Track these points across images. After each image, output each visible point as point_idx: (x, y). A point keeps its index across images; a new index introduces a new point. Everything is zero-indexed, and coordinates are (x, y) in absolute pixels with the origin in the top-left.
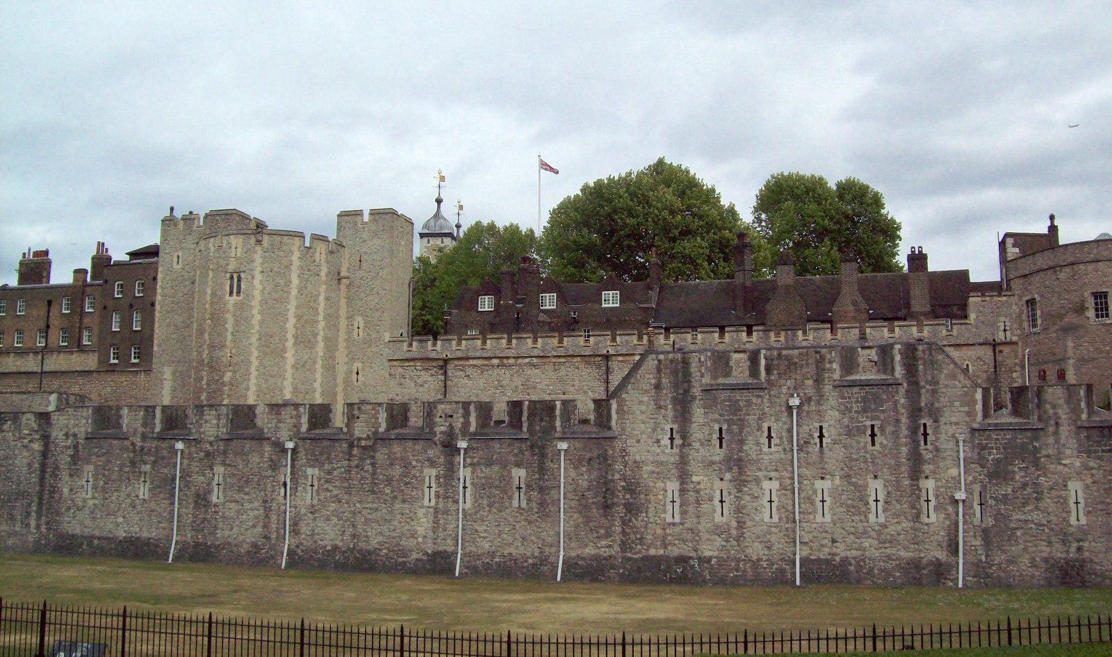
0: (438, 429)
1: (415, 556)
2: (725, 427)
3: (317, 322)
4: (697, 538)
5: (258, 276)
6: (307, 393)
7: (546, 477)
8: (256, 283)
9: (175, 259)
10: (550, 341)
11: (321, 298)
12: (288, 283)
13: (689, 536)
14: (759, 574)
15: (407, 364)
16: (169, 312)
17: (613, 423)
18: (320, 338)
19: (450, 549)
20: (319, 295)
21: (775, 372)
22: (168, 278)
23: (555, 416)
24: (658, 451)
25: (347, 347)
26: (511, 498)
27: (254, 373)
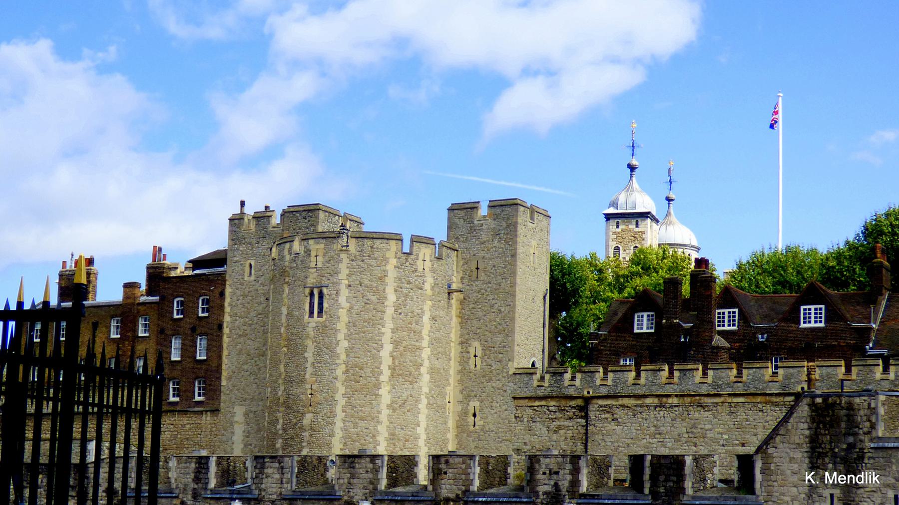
0: (542, 489)
3: (420, 349)
5: (344, 292)
6: (407, 441)
8: (342, 300)
9: (247, 269)
10: (723, 373)
11: (426, 318)
12: (382, 299)
15: (537, 403)
16: (240, 336)
17: (757, 486)
18: (423, 370)
20: (423, 313)
22: (238, 292)
25: (461, 381)
27: (340, 415)
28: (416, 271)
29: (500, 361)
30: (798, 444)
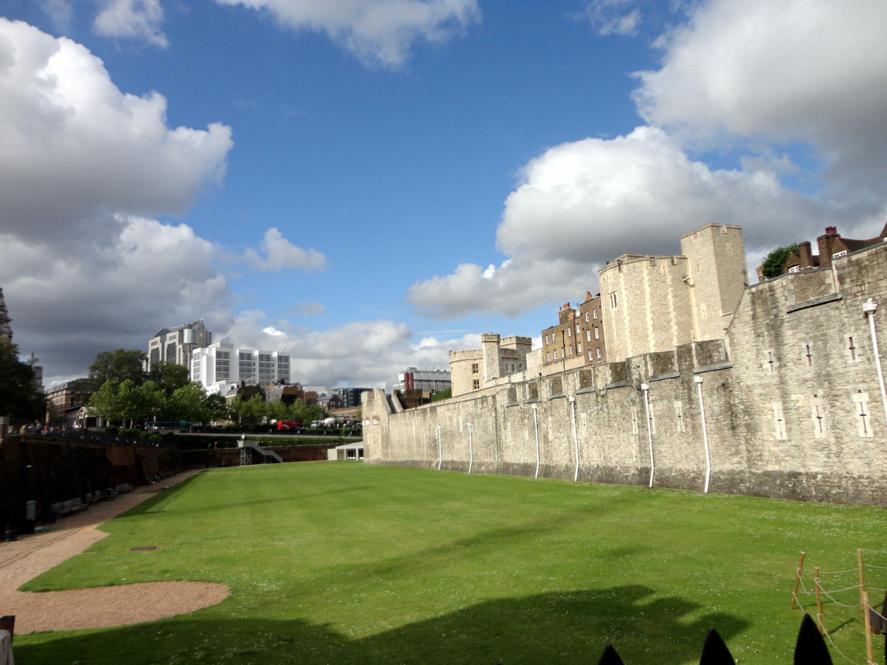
1: (633, 471)
2: (811, 345)
3: (669, 313)
4: (803, 455)
5: (624, 292)
7: (694, 406)
11: (670, 297)
12: (643, 291)
13: (793, 451)
14: (860, 491)
18: (672, 324)
19: (649, 467)
20: (668, 295)
21: (848, 280)
23: (692, 356)
24: (763, 375)
26: (676, 424)
28: (660, 274)
29: (715, 311)
30: (747, 322)
